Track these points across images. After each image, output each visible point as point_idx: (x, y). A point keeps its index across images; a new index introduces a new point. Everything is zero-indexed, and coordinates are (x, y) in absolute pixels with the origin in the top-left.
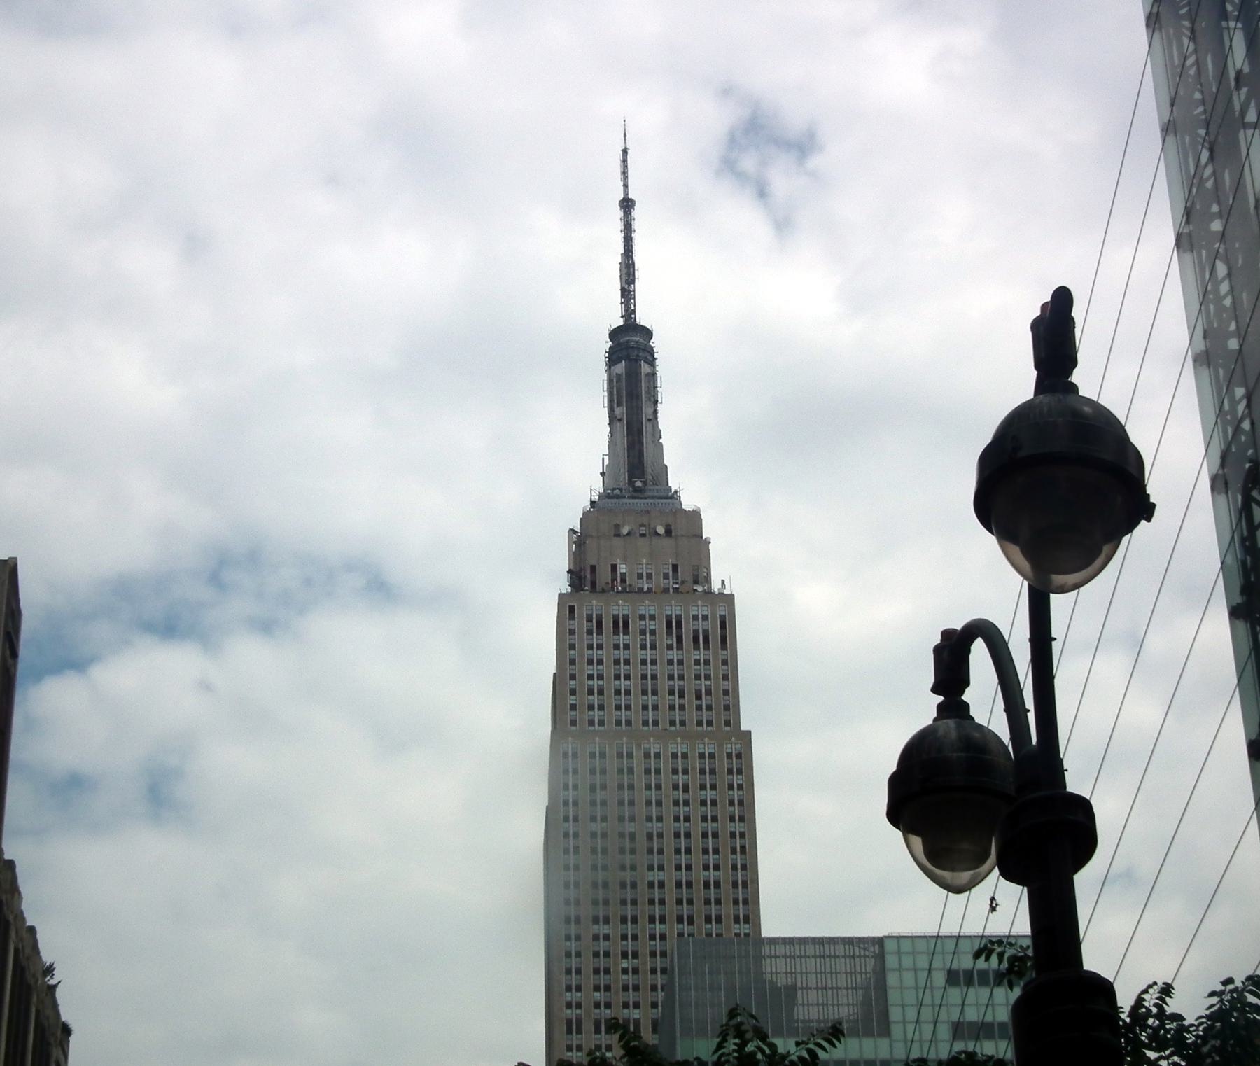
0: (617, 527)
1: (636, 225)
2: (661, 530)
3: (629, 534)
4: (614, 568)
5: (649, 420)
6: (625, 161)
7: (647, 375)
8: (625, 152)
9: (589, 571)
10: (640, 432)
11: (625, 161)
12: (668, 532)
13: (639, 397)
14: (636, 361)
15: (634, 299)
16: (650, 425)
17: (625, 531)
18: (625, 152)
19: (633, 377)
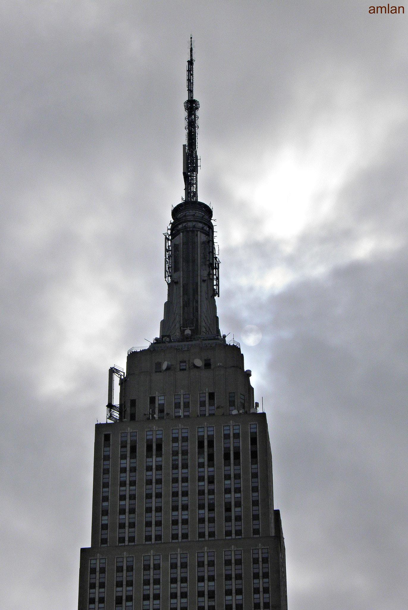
0: (159, 365)
1: (200, 122)
2: (199, 363)
3: (168, 368)
4: (152, 400)
5: (204, 281)
6: (190, 71)
7: (204, 243)
8: (191, 63)
9: (128, 405)
10: (195, 291)
11: (190, 71)
12: (207, 365)
13: (194, 261)
14: (193, 231)
15: (196, 184)
16: (204, 285)
17: (164, 366)
18: (191, 63)
19: (190, 244)
